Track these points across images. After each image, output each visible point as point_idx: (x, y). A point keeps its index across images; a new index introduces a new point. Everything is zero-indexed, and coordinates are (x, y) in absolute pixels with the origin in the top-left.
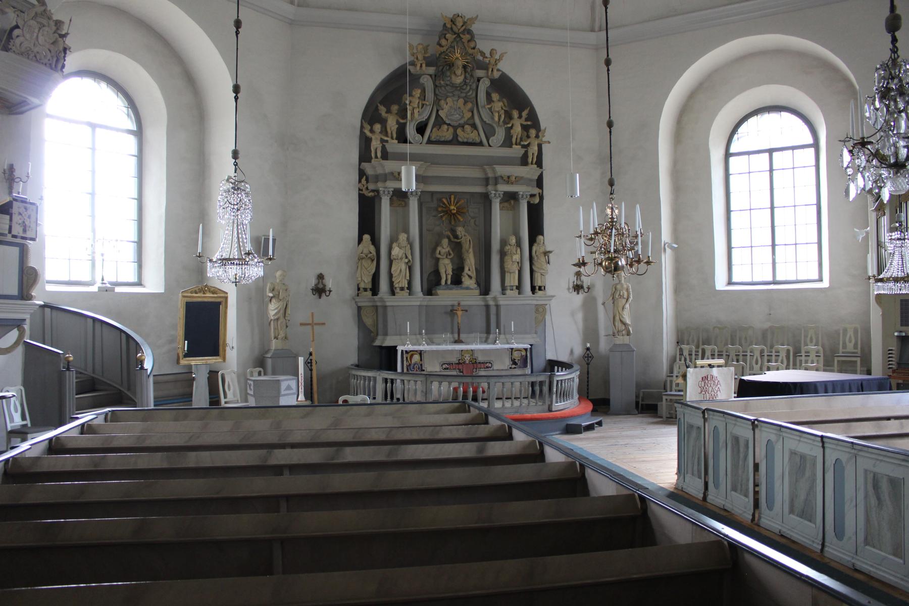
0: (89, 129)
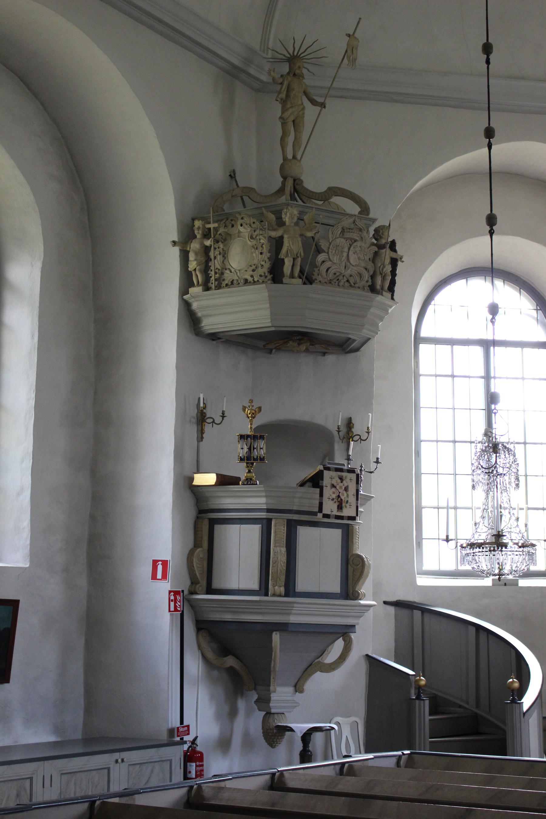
0: (478, 351)
